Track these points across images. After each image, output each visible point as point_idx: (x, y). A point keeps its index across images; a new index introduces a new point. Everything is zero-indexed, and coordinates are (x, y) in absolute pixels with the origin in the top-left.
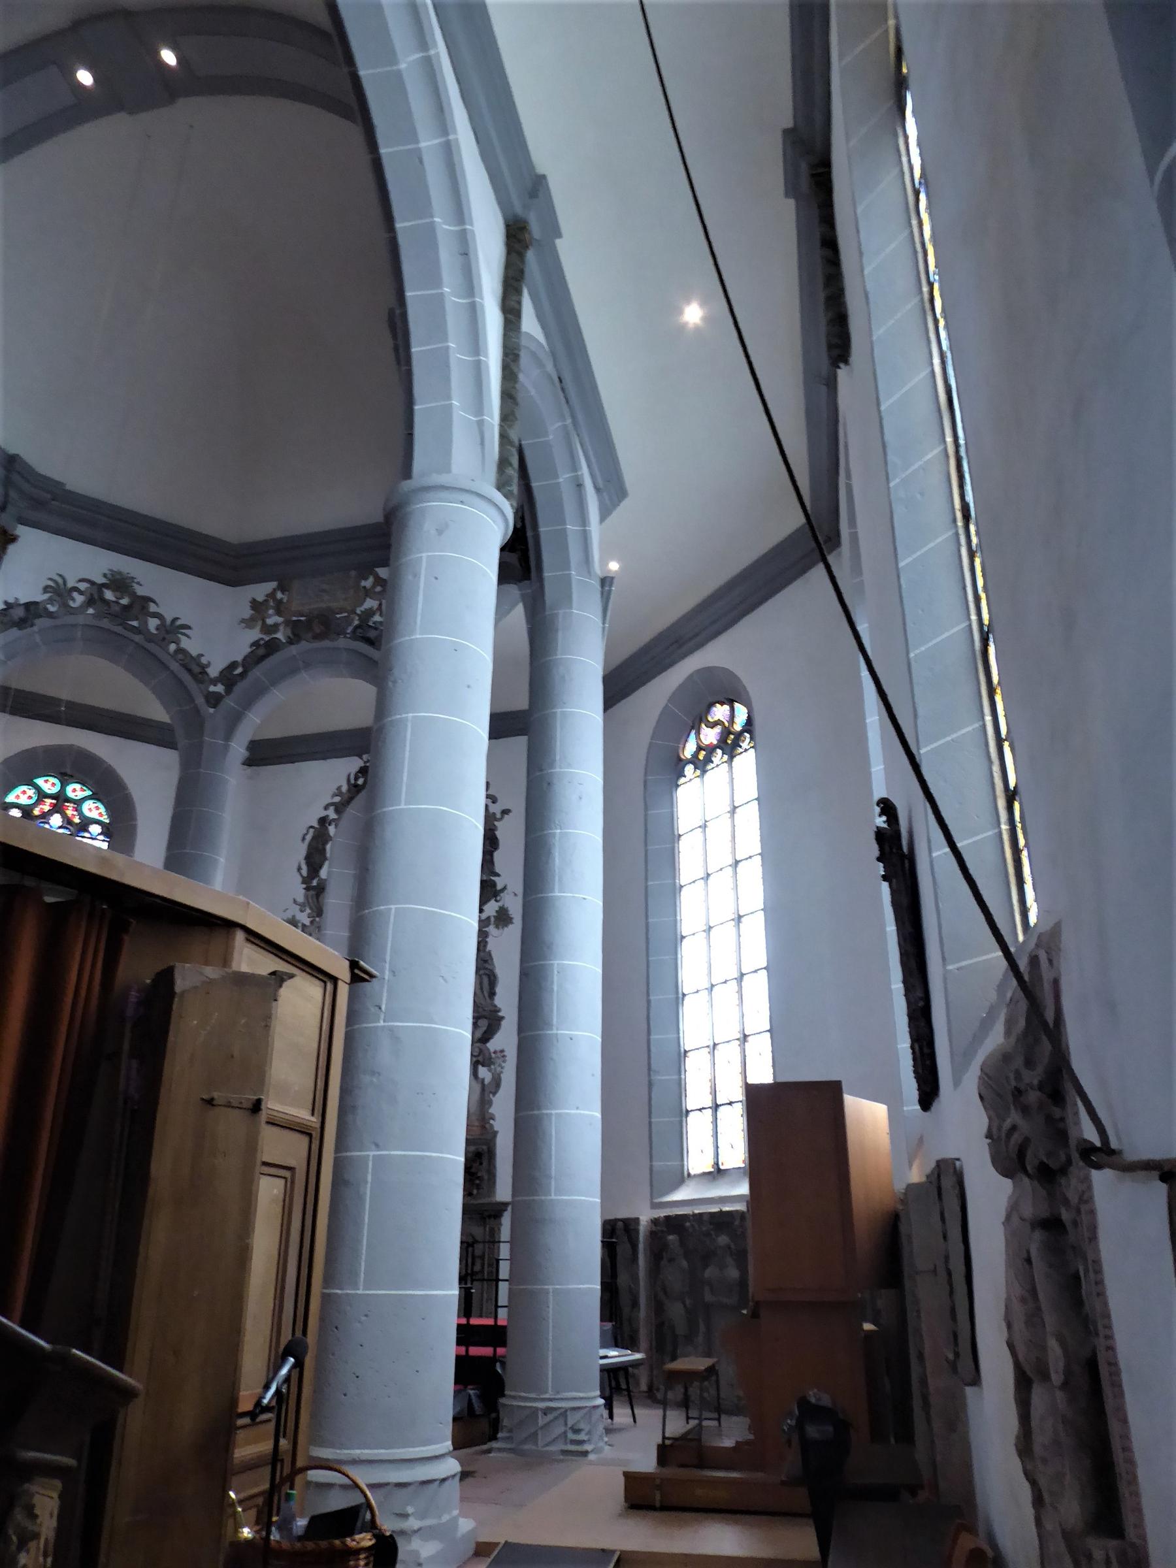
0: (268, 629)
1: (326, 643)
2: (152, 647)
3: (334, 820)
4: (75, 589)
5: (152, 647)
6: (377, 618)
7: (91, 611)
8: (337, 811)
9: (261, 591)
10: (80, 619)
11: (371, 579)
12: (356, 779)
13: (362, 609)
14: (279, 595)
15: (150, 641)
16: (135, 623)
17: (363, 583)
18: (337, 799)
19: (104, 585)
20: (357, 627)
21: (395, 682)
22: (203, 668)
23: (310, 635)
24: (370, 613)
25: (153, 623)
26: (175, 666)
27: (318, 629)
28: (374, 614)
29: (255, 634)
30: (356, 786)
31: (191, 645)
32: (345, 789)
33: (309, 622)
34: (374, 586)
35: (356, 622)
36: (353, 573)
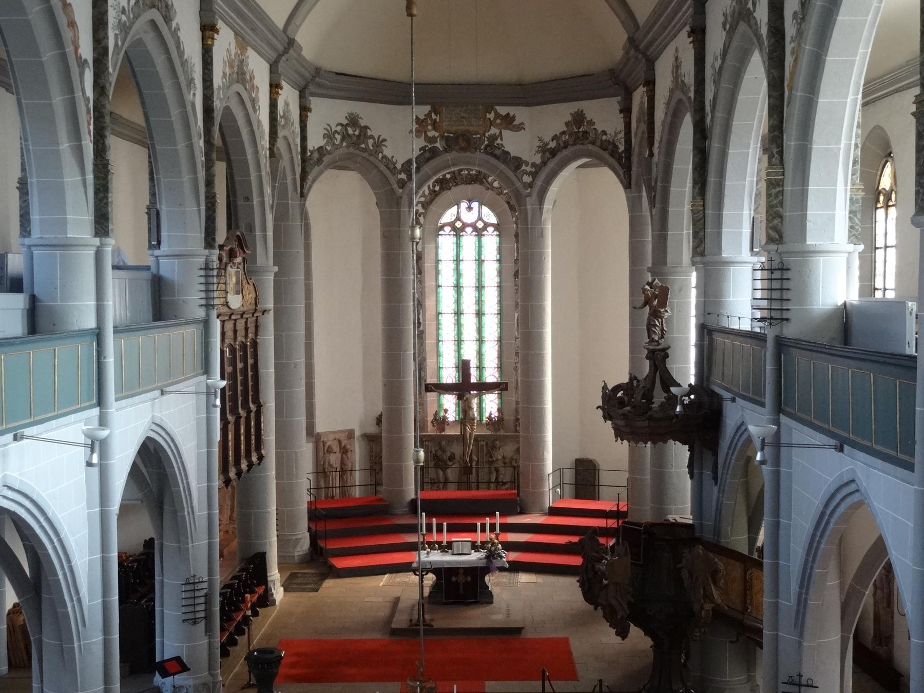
0: (432, 140)
1: (468, 154)
2: (372, 159)
3: (422, 213)
4: (336, 132)
5: (372, 159)
6: (499, 141)
7: (344, 144)
8: (423, 207)
9: (422, 111)
10: (341, 151)
11: (493, 114)
12: (434, 187)
14: (434, 116)
15: (371, 155)
16: (363, 146)
17: (488, 116)
18: (423, 199)
19: (347, 125)
20: (487, 146)
22: (394, 164)
24: (493, 138)
25: (371, 142)
26: (382, 168)
28: (497, 139)
29: (421, 142)
30: (435, 191)
31: (388, 152)
32: (427, 192)
33: (457, 137)
34: (495, 119)
36: (481, 107)
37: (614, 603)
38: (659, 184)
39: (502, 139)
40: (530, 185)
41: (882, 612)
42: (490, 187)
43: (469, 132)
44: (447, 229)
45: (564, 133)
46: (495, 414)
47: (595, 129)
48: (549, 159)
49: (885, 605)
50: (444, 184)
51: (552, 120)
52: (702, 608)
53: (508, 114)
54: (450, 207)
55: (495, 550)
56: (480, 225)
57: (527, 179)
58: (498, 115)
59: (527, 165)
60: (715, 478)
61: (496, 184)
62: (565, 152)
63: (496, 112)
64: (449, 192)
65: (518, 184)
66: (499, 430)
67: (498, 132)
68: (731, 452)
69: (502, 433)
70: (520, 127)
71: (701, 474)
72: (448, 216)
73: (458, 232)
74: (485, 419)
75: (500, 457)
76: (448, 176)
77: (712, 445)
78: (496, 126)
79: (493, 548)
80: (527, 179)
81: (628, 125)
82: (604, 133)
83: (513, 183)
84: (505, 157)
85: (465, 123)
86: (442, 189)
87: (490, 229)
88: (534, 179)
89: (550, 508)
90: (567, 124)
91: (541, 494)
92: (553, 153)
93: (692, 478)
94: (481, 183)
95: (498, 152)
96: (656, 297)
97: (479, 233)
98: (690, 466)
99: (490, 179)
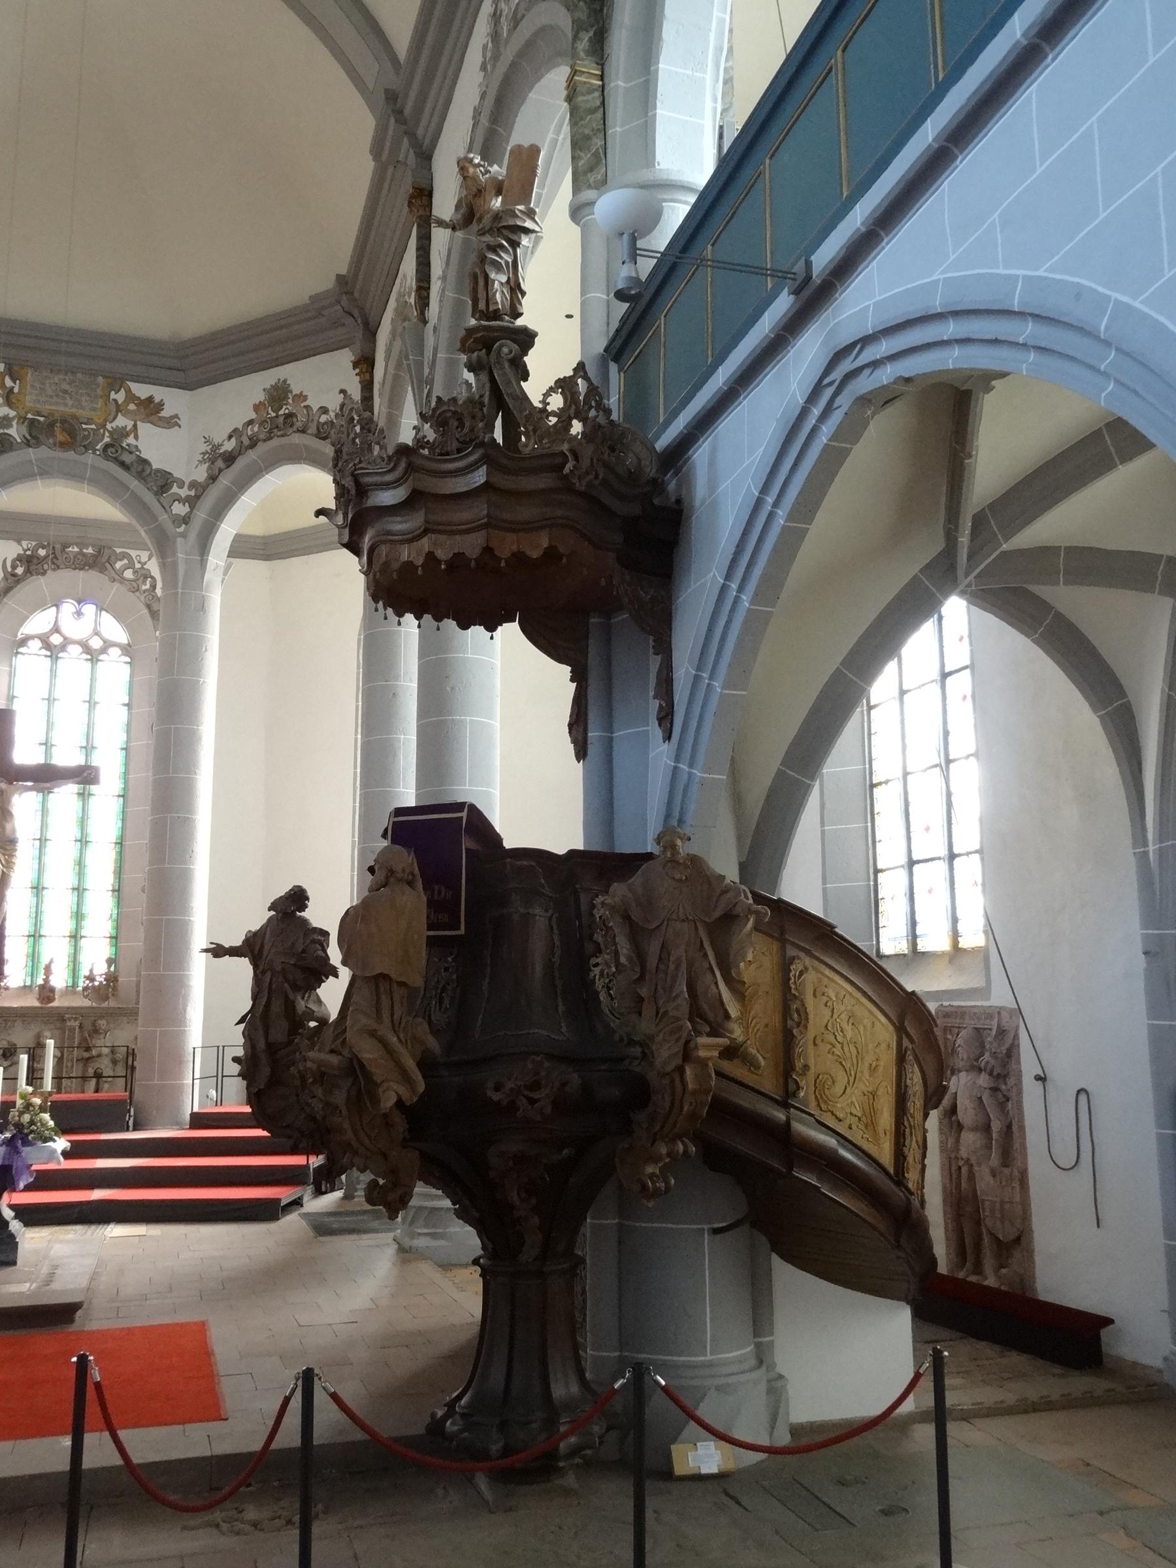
1: (71, 455)
6: (131, 440)
12: (14, 567)
13: (114, 425)
14: (8, 382)
17: (113, 395)
20: (107, 446)
21: (452, 688)
23: (51, 441)
24: (122, 433)
27: (61, 437)
28: (128, 435)
30: (14, 575)
33: (51, 425)
35: (107, 440)
36: (100, 379)
37: (369, 1052)
38: (441, 355)
39: (136, 438)
40: (186, 520)
41: (985, 1182)
42: (119, 577)
43: (74, 417)
44: (35, 645)
45: (251, 422)
46: (101, 969)
47: (307, 407)
48: (220, 471)
49: (995, 1160)
50: (31, 564)
51: (234, 403)
52: (687, 1054)
53: (150, 399)
54: (41, 605)
55: (32, 1122)
56: (96, 643)
57: (180, 509)
58: (130, 397)
59: (181, 486)
60: (666, 717)
61: (129, 574)
62: (252, 455)
63: (128, 391)
64: (41, 581)
65: (163, 517)
66: (107, 998)
67: (130, 424)
68: (734, 586)
69: (112, 1003)
70: (172, 422)
71: (608, 745)
72: (39, 622)
73: (53, 651)
74: (82, 983)
75: (106, 1051)
76: (42, 552)
77: (658, 625)
78: (127, 414)
79: (26, 1118)
80: (180, 509)
81: (367, 386)
82: (324, 410)
83: (154, 518)
84: (140, 468)
85: (70, 403)
86: (28, 572)
87: (115, 652)
88: (192, 507)
89: (193, 1115)
90: (257, 408)
91: (178, 1090)
92: (230, 459)
93: (581, 753)
94: (102, 570)
95: (127, 458)
96: (499, 192)
97: (93, 656)
98: (578, 724)
99: (118, 565)
